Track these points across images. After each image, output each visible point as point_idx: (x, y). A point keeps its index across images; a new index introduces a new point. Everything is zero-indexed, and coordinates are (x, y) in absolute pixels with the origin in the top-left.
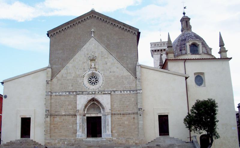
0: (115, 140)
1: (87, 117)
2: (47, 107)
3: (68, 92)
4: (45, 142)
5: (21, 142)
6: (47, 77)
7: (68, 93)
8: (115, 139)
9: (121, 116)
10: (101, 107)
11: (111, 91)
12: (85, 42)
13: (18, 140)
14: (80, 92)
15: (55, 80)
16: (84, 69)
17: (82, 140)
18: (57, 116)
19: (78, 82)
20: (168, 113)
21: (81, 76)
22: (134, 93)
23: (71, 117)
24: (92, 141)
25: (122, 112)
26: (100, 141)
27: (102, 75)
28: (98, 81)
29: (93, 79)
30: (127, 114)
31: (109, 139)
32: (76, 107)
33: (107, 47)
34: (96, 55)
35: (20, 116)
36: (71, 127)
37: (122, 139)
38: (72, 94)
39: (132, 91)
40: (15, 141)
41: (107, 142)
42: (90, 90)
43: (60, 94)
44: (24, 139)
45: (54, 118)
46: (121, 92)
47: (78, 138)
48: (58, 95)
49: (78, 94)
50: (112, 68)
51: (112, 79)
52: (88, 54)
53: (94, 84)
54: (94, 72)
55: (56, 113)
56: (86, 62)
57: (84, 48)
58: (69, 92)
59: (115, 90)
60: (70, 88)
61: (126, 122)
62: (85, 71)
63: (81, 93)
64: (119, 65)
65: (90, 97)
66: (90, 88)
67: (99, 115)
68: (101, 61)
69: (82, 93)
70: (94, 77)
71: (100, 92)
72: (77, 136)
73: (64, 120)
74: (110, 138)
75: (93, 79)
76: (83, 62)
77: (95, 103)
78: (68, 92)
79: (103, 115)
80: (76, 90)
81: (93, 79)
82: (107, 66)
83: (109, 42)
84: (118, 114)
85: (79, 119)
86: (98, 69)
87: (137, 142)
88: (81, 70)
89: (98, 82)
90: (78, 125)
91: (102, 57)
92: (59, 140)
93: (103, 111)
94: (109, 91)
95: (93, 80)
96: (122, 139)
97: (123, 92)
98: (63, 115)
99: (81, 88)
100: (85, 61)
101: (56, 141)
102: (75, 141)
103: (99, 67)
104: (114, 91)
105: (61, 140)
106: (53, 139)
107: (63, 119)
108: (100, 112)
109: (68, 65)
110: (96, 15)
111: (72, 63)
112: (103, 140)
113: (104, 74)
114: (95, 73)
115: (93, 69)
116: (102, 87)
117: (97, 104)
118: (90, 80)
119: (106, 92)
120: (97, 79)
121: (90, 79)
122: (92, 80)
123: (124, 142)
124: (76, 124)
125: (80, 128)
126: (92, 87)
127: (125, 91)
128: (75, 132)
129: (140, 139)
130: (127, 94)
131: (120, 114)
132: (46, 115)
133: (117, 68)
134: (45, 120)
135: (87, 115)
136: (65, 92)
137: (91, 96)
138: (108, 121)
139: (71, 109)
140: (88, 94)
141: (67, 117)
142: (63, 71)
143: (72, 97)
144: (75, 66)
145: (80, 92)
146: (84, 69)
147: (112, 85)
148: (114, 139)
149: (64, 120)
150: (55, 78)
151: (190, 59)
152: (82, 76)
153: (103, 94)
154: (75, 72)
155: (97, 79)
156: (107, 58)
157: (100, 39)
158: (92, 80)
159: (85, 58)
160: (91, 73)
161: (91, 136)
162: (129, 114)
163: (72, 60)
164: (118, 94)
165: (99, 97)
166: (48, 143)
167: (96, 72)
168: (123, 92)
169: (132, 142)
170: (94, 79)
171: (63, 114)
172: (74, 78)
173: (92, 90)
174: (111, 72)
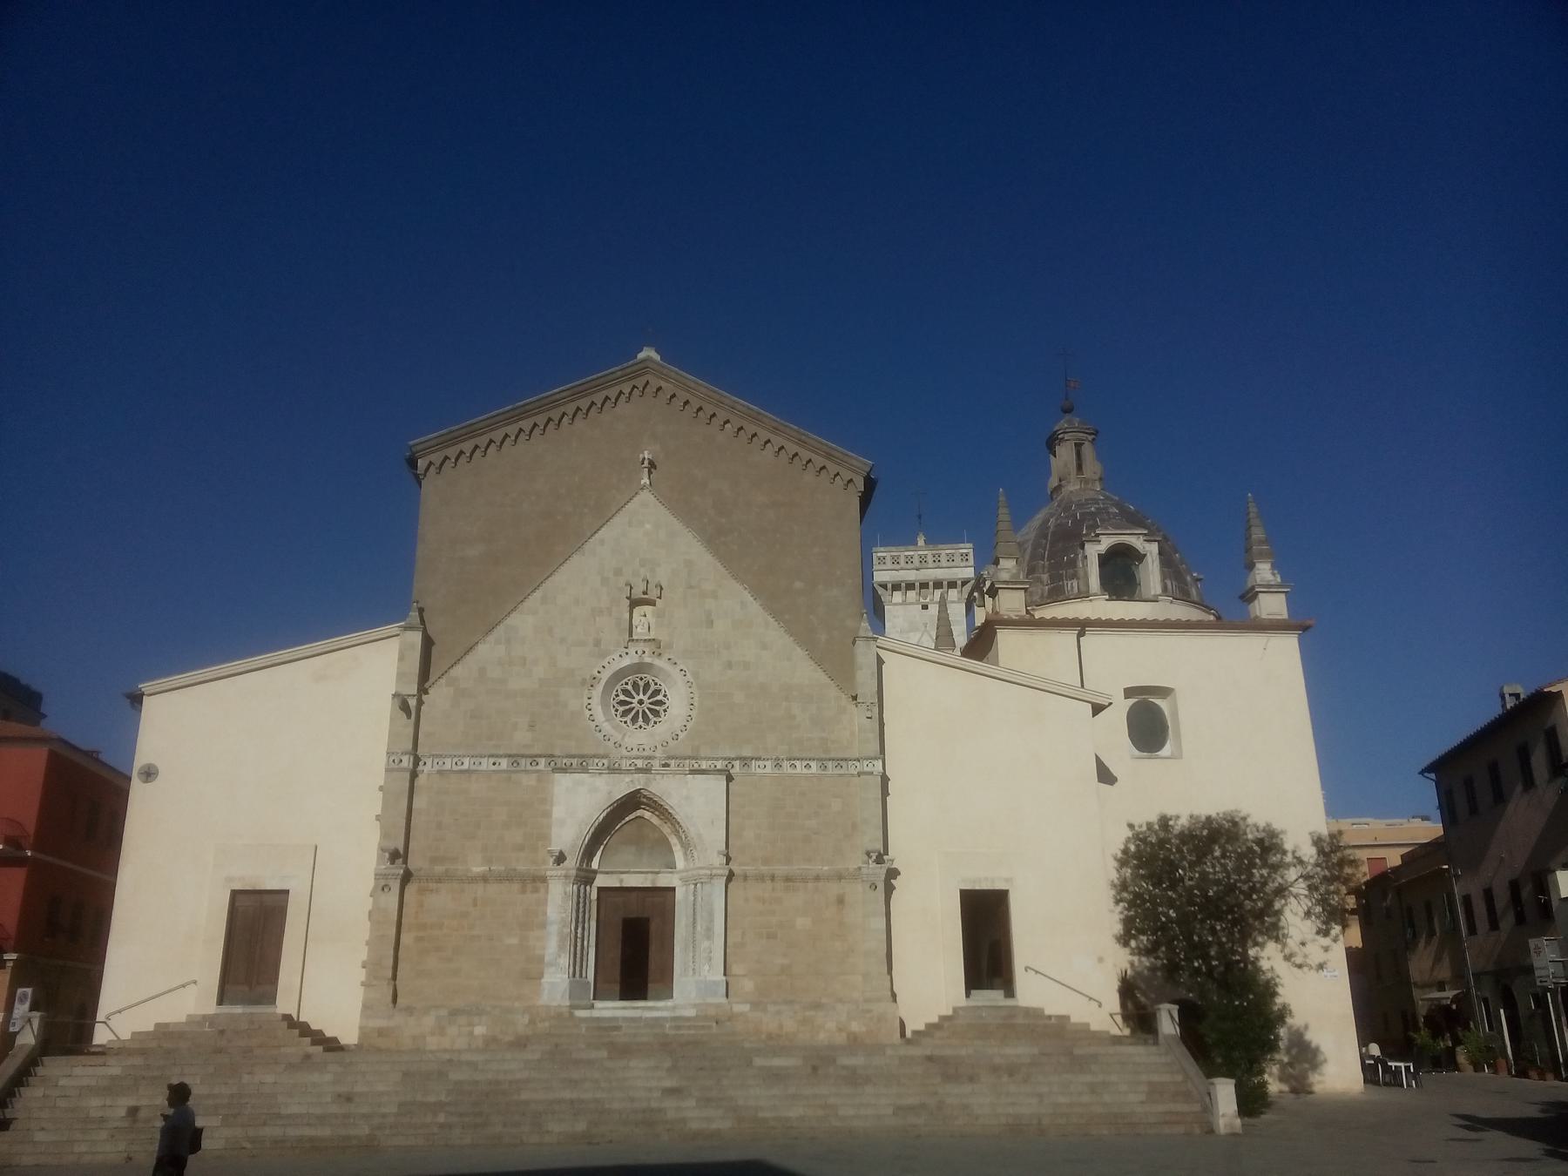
0: (741, 1014)
1: (600, 889)
2: (385, 835)
3: (510, 756)
4: (361, 1028)
5: (222, 1032)
6: (401, 676)
7: (504, 764)
8: (746, 1008)
9: (773, 889)
10: (673, 840)
11: (730, 759)
12: (603, 513)
13: (204, 1017)
14: (573, 757)
15: (439, 695)
16: (597, 643)
17: (571, 1014)
18: (439, 881)
20: (1007, 880)
22: (842, 772)
23: (516, 886)
24: (625, 1019)
25: (780, 869)
26: (665, 1019)
27: (689, 677)
28: (665, 707)
29: (641, 696)
30: (804, 880)
31: (712, 1012)
32: (545, 838)
33: (714, 539)
34: (662, 576)
35: (229, 879)
36: (514, 941)
37: (779, 1013)
38: (529, 767)
39: (830, 764)
40: (187, 1023)
41: (703, 1027)
42: (625, 753)
43: (466, 766)
44: (238, 1010)
45: (421, 891)
46: (778, 766)
47: (548, 1007)
48: (451, 771)
49: (564, 770)
52: (618, 572)
53: (646, 720)
54: (647, 660)
55: (439, 869)
57: (602, 542)
58: (514, 758)
59: (747, 753)
60: (521, 738)
61: (802, 922)
62: (603, 655)
63: (575, 761)
64: (776, 635)
65: (622, 786)
67: (663, 881)
69: (581, 763)
70: (647, 686)
71: (672, 762)
72: (546, 992)
73: (475, 905)
74: (718, 1006)
75: (641, 696)
77: (647, 815)
78: (510, 756)
79: (685, 881)
81: (637, 698)
83: (724, 520)
84: (761, 878)
85: (558, 899)
86: (670, 646)
87: (855, 1027)
90: (553, 929)
91: (691, 587)
92: (443, 1012)
93: (686, 860)
94: (717, 759)
95: (641, 702)
96: (779, 1013)
97: (786, 764)
98: (473, 880)
101: (429, 1021)
102: (532, 1022)
104: (746, 761)
105: (454, 1013)
106: (410, 1010)
107: (475, 900)
108: (671, 865)
109: (515, 620)
110: (663, 384)
112: (678, 1013)
113: (696, 675)
114: (650, 665)
115: (640, 647)
117: (655, 820)
118: (622, 703)
119: (704, 765)
120: (660, 697)
122: (635, 701)
123: (790, 1025)
124: (543, 925)
125: (561, 948)
126: (638, 738)
127: (798, 763)
128: (532, 975)
129: (869, 1011)
130: (807, 777)
131: (773, 878)
132: (378, 876)
133: (764, 646)
134: (375, 903)
135: (601, 881)
136: (492, 756)
137: (627, 778)
138: (711, 915)
139: (521, 848)
140: (613, 770)
141: (493, 889)
142: (488, 651)
143: (529, 781)
145: (573, 757)
146: (597, 643)
148: (738, 1008)
149: (475, 905)
150: (443, 681)
151: (1115, 618)
152: (584, 682)
153: (694, 772)
155: (660, 697)
157: (682, 505)
158: (635, 701)
161: (617, 988)
162: (817, 878)
163: (538, 594)
164: (763, 776)
165: (673, 790)
166: (379, 1036)
167: (657, 662)
168: (786, 764)
169: (831, 1025)
170: (645, 698)
171: (478, 869)
173: (635, 752)
174: (729, 665)
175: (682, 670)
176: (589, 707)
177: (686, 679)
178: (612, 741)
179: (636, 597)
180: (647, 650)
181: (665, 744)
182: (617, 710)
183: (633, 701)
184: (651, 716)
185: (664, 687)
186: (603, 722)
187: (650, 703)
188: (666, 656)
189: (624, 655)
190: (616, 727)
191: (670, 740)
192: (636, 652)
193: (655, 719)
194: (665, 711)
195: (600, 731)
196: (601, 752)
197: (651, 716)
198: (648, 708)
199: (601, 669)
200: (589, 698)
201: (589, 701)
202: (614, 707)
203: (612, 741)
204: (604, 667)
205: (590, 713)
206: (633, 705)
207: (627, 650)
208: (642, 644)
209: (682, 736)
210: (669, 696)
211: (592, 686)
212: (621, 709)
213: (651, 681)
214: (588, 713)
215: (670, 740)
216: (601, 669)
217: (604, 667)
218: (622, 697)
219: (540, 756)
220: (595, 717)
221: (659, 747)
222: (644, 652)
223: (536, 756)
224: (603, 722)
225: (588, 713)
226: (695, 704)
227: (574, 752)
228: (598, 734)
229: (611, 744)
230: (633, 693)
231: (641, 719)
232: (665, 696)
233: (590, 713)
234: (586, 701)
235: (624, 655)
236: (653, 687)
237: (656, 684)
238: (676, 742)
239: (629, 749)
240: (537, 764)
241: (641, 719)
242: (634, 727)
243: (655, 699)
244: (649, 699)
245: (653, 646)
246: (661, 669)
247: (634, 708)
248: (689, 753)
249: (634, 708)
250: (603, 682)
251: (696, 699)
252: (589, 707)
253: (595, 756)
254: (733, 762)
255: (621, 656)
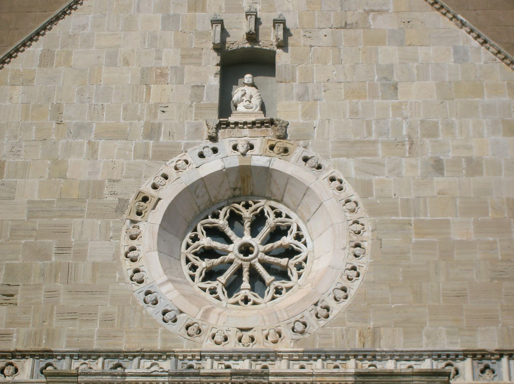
19: (81, 255)
21: (113, 200)
27: (349, 190)
28: (300, 258)
42: (208, 345)
50: (449, 126)
51: (456, 235)
56: (179, 72)
66: (213, 319)
68: (338, 61)
75: (247, 238)
76: (145, 72)
80: (51, 335)
82: (397, 109)
88: (119, 143)
89: (293, 272)
95: (246, 249)
99: (107, 320)
100: (164, 64)
103: (308, 114)
111: (29, 82)
114: (267, 171)
116: (349, 309)
120: (287, 240)
121: (206, 241)
122: (233, 248)
144: (58, 109)
147: (460, 295)
154: (56, 162)
155: (287, 240)
156: (401, 43)
159: (170, 36)
160: (225, 173)
170: (256, 242)
172: (32, 214)
173: (232, 345)
175: (332, 179)
176: (131, 254)
177: (343, 195)
178: (182, 320)
179: (235, 47)
180: (257, 143)
181: (299, 327)
182: (194, 268)
183: (230, 247)
184: (268, 277)
185: (295, 221)
186: (162, 284)
187: (267, 253)
188: (298, 152)
189: (208, 152)
190: (190, 298)
191: (311, 320)
192: (235, 148)
193: (277, 283)
194: (299, 267)
195: (155, 302)
196: (159, 346)
197: (268, 277)
198: (267, 266)
199: (159, 180)
200: (133, 238)
201: (134, 243)
202: (188, 261)
203: (182, 320)
204: (166, 177)
205: (135, 265)
206: (230, 256)
207: (215, 145)
208: (246, 131)
209: (336, 309)
210: (307, 237)
211: (139, 214)
212: (203, 264)
213: (267, 209)
214: (128, 266)
215: (311, 320)
216: (159, 180)
217: (166, 177)
218: (206, 241)
219: (23, 355)
220: (145, 274)
221: (287, 333)
222: (252, 147)
223: (14, 354)
224: (162, 284)
225: (128, 266)
226: (365, 245)
227: (95, 347)
228: (151, 309)
229: (178, 328)
230: (229, 232)
231: (246, 284)
232: (298, 237)
233: (135, 265)
234: (125, 243)
235: (208, 152)
236: (271, 221)
237: (278, 215)
238: (322, 322)
239: (219, 338)
240: (16, 370)
241: (246, 284)
242: (232, 300)
243: (278, 243)
244: (265, 242)
245: (270, 132)
246: (289, 178)
247: (231, 262)
248: (357, 345)
249: (231, 262)
250: (163, 207)
251: (367, 234)
252: (131, 254)
253: (143, 355)
254: (459, 364)
255: (201, 155)
